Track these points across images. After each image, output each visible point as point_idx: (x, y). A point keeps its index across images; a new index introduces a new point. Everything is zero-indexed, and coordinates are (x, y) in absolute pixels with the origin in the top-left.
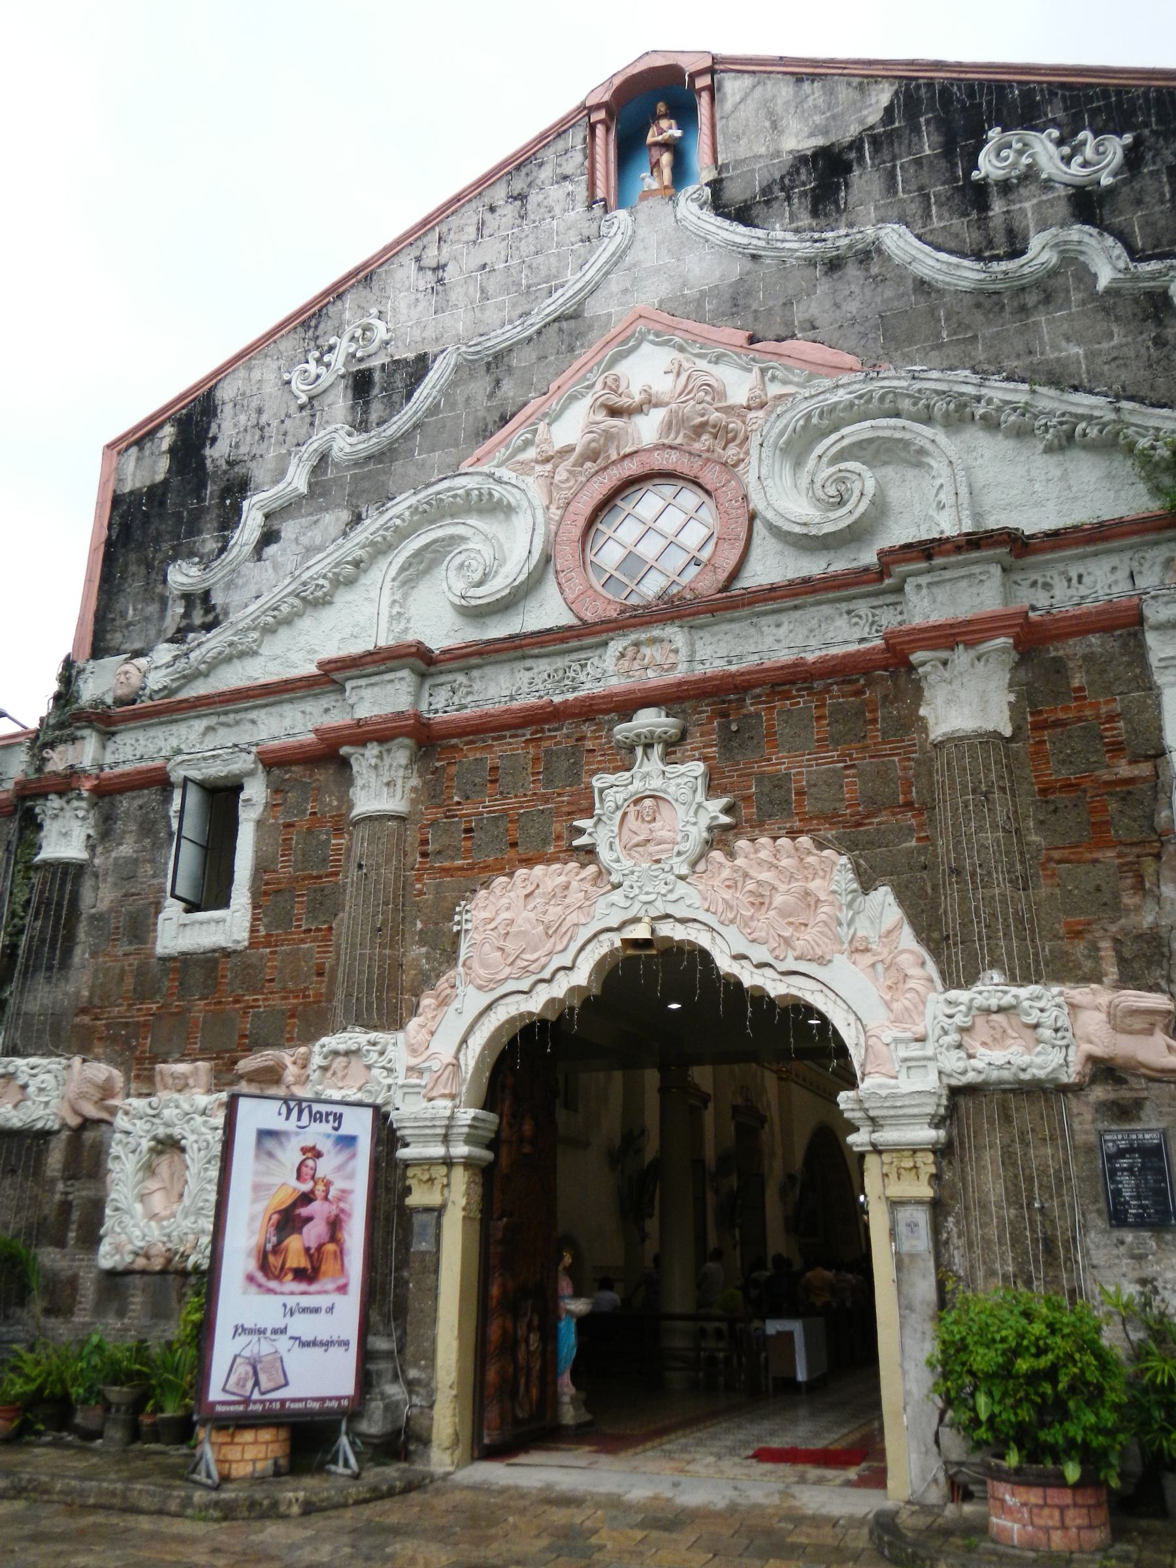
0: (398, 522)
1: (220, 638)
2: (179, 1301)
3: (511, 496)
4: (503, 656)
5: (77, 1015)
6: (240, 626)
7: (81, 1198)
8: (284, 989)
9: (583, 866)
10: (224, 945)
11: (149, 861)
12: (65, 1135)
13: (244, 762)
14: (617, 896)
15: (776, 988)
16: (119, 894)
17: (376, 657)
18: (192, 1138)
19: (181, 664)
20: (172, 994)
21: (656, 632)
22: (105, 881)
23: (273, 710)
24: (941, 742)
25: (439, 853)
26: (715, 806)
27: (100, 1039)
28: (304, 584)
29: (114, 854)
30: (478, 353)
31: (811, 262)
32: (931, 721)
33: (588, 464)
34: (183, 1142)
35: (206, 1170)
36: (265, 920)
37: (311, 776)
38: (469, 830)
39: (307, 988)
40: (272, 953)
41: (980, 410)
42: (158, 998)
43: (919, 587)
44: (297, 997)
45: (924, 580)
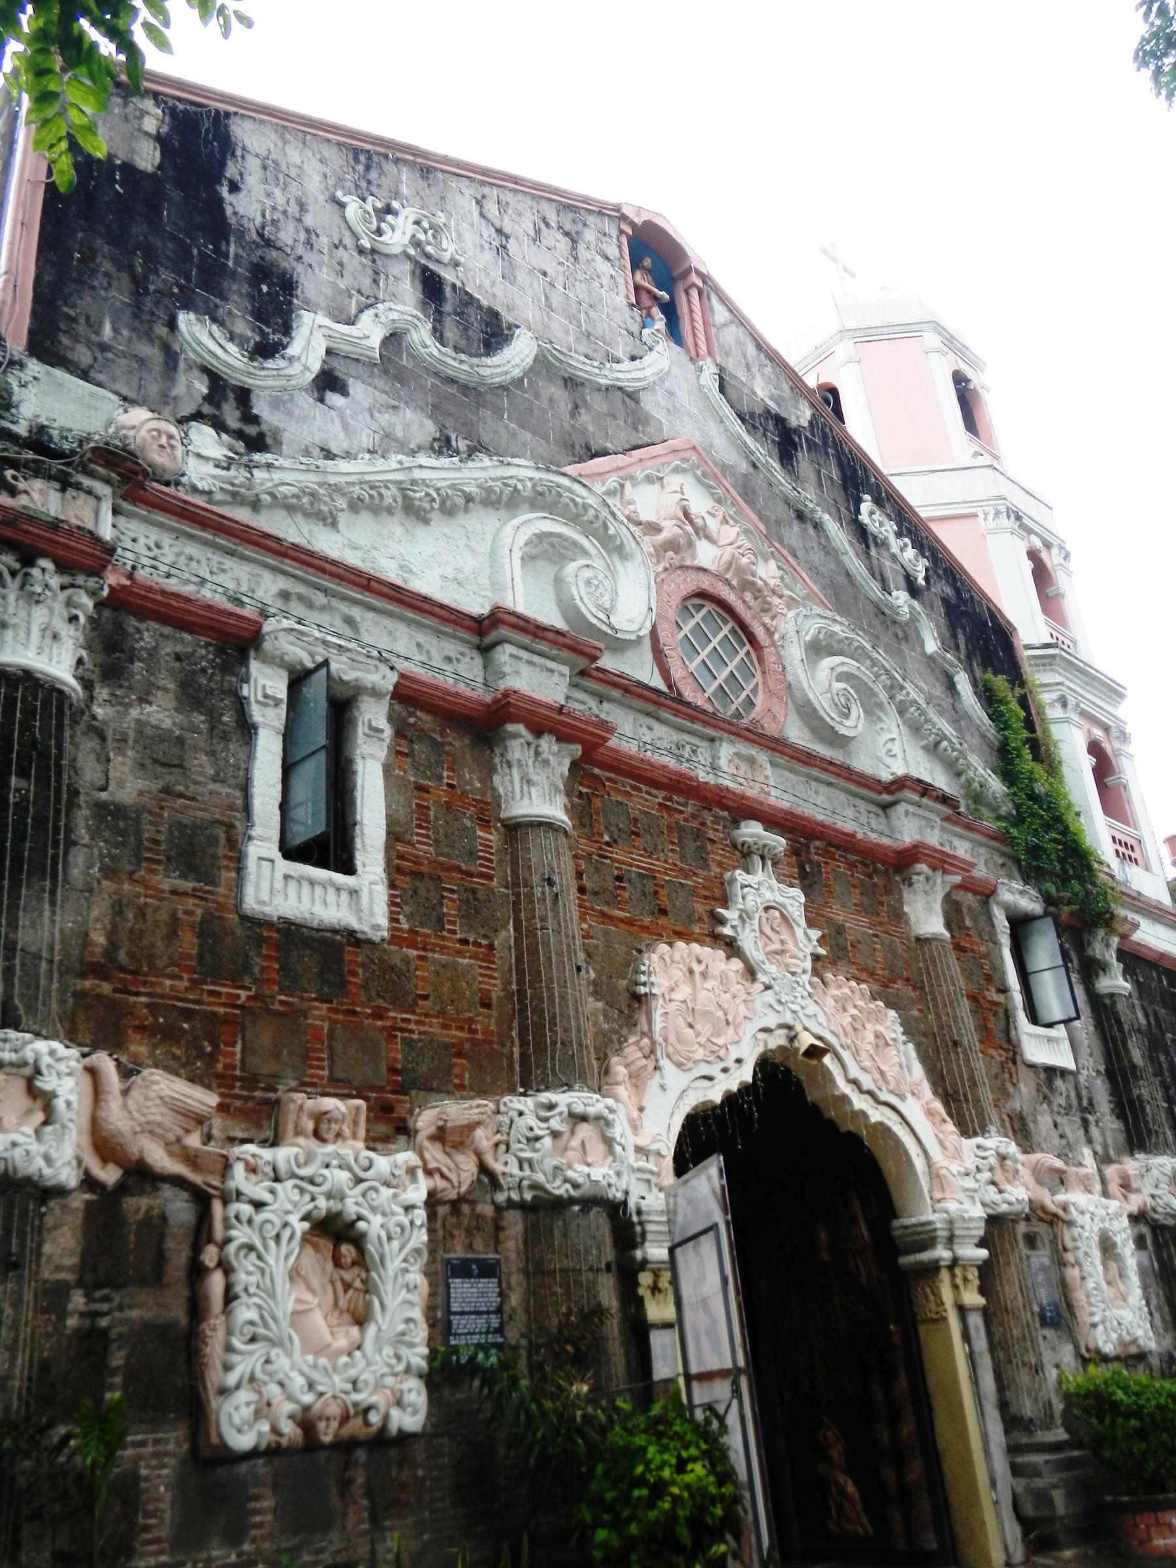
0: (520, 487)
1: (301, 477)
2: (342, 1495)
3: (630, 544)
4: (637, 703)
5: (83, 975)
6: (332, 480)
7: (128, 1321)
8: (442, 1013)
9: (728, 958)
10: (355, 924)
11: (206, 753)
12: (78, 1201)
13: (387, 680)
14: (769, 996)
15: (876, 1115)
16: (156, 786)
17: (561, 639)
18: (377, 1220)
19: (238, 475)
20: (269, 981)
21: (753, 751)
22: (121, 751)
23: (387, 622)
24: (927, 939)
25: (596, 893)
26: (815, 934)
27: (141, 1029)
28: (414, 482)
29: (134, 713)
30: (561, 361)
31: (787, 502)
32: (913, 919)
33: (671, 553)
34: (362, 1225)
35: (406, 1271)
36: (407, 909)
37: (442, 734)
38: (619, 878)
39: (471, 1021)
40: (420, 958)
41: (900, 697)
42: (247, 981)
43: (907, 813)
44: (461, 1028)
45: (911, 808)
